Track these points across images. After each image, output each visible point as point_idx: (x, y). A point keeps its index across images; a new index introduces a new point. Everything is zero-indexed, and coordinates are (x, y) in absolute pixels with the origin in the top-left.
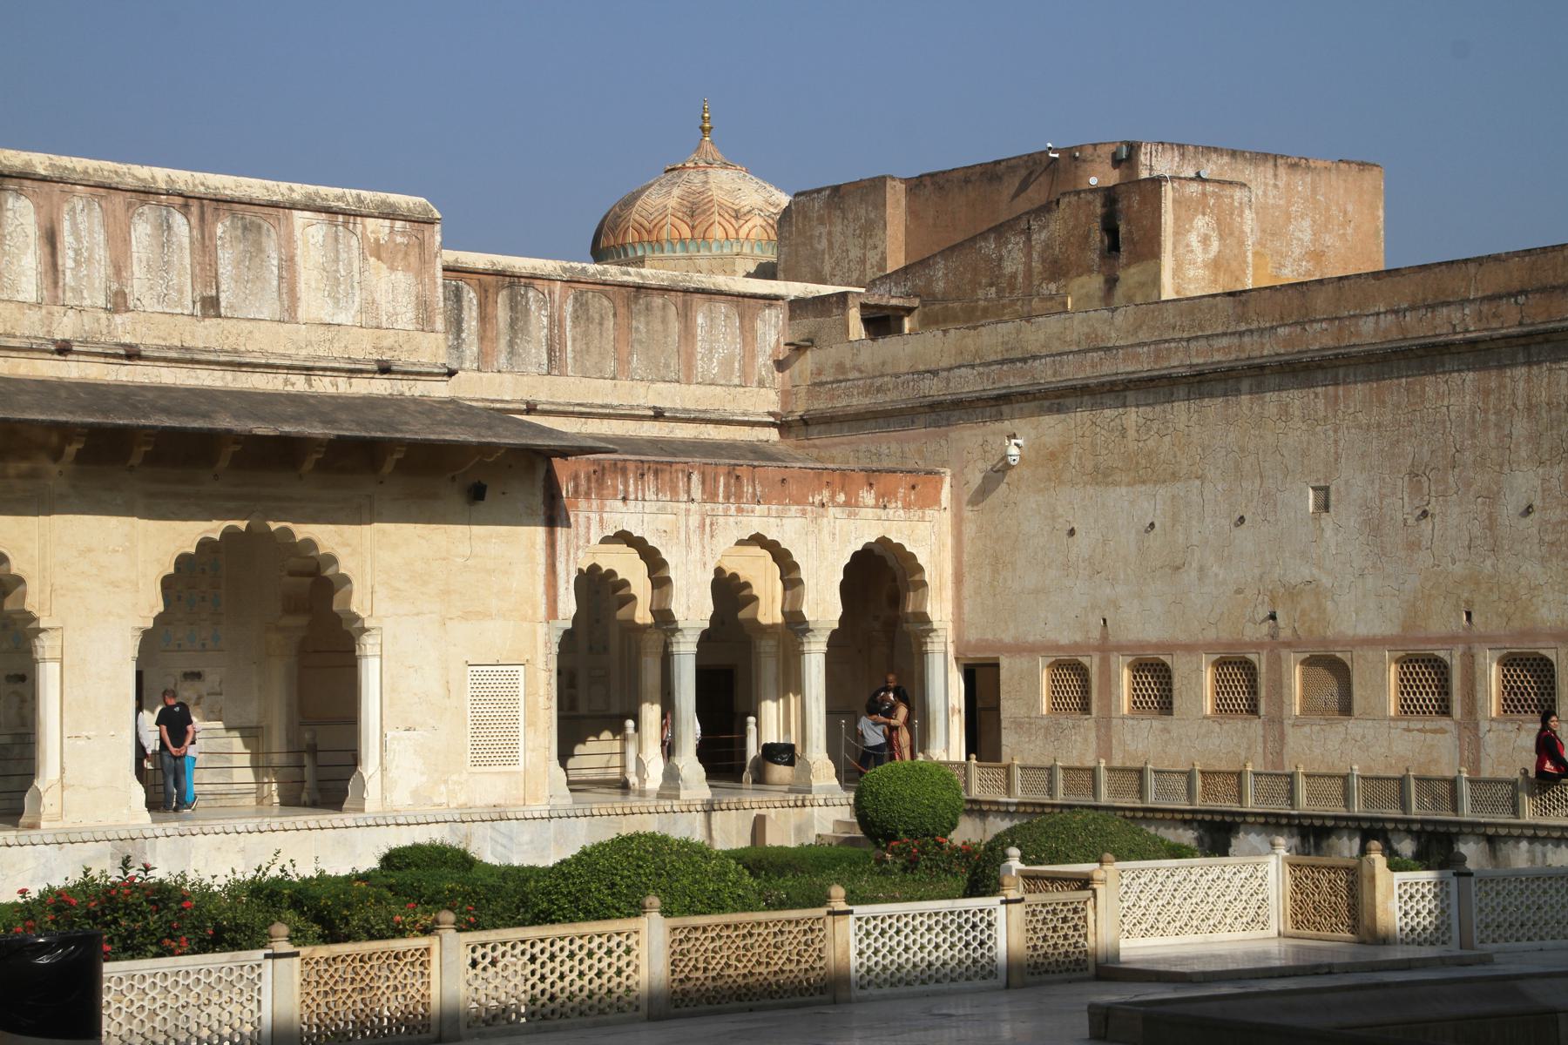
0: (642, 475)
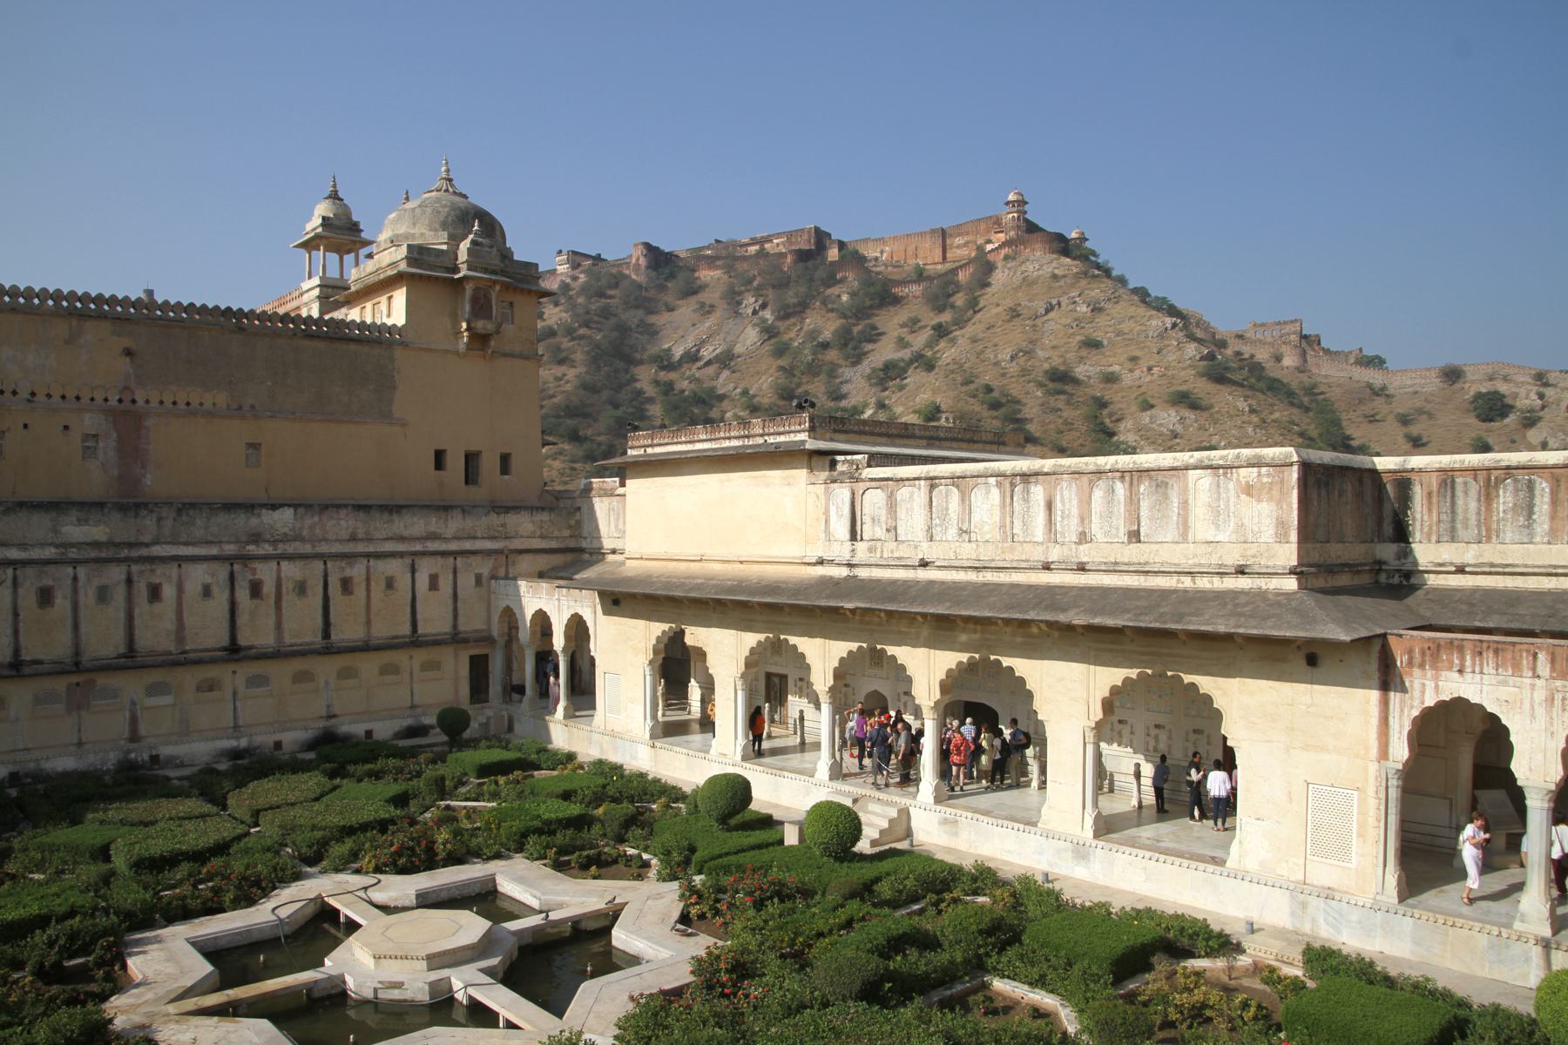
0: (1480, 653)
